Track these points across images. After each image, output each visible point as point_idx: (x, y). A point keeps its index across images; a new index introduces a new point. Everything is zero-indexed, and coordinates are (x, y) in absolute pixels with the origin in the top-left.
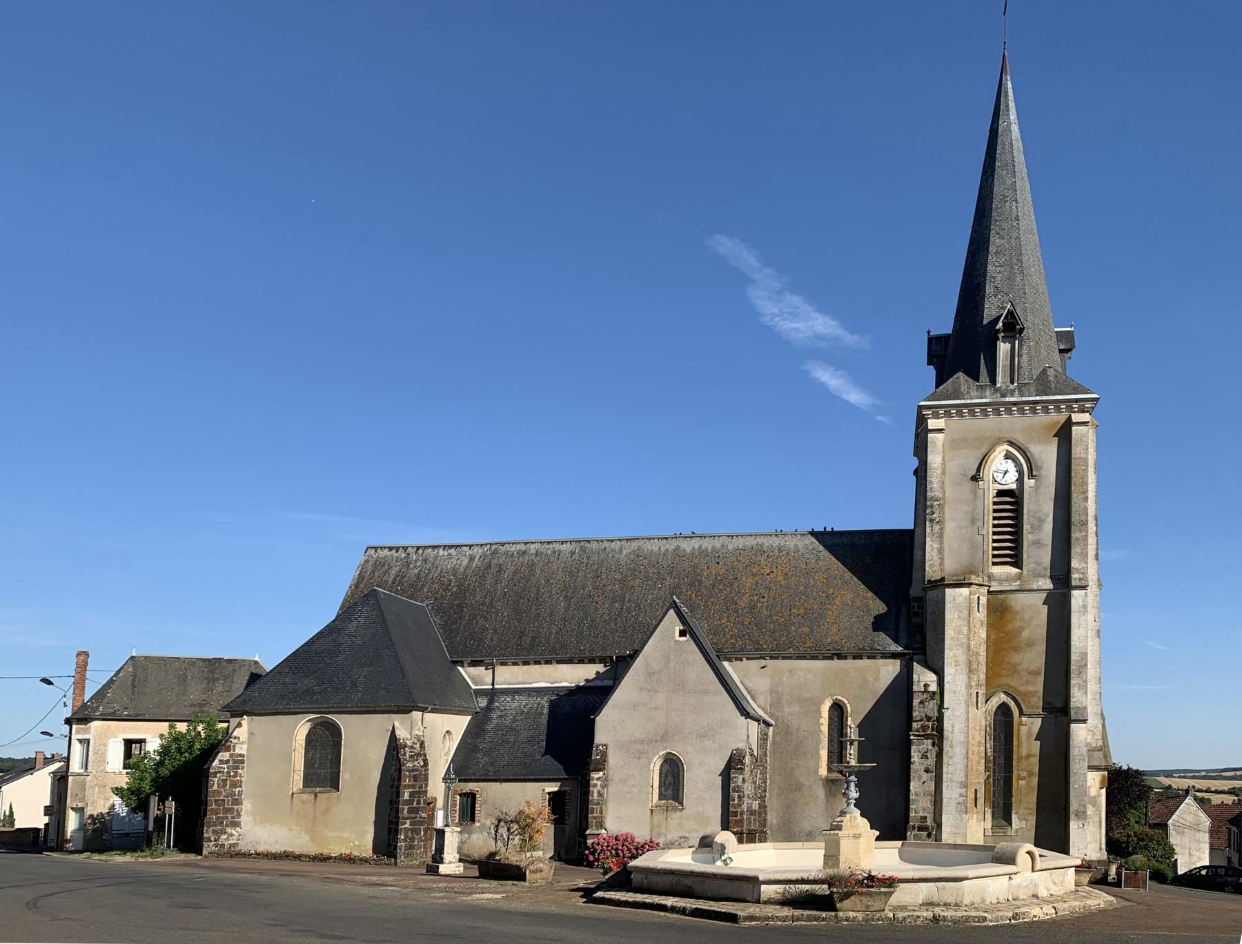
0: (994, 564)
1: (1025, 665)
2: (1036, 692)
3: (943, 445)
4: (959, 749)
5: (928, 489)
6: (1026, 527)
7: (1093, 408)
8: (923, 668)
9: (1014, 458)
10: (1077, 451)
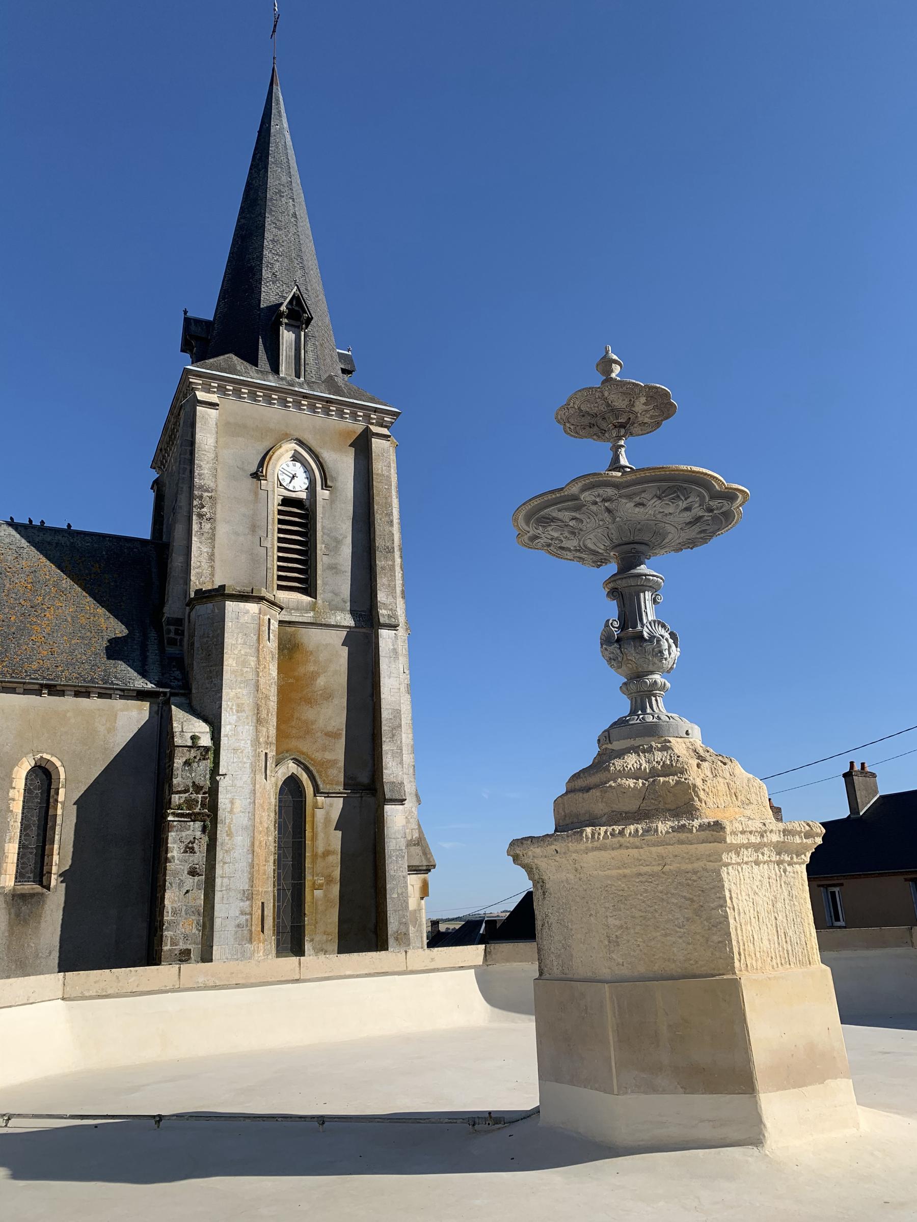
0: (280, 588)
1: (321, 723)
2: (335, 762)
3: (216, 424)
4: (240, 838)
5: (196, 474)
6: (320, 547)
7: (392, 423)
8: (186, 714)
9: (304, 461)
10: (378, 466)
